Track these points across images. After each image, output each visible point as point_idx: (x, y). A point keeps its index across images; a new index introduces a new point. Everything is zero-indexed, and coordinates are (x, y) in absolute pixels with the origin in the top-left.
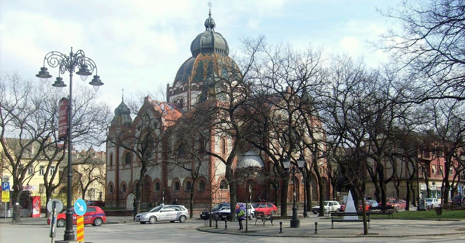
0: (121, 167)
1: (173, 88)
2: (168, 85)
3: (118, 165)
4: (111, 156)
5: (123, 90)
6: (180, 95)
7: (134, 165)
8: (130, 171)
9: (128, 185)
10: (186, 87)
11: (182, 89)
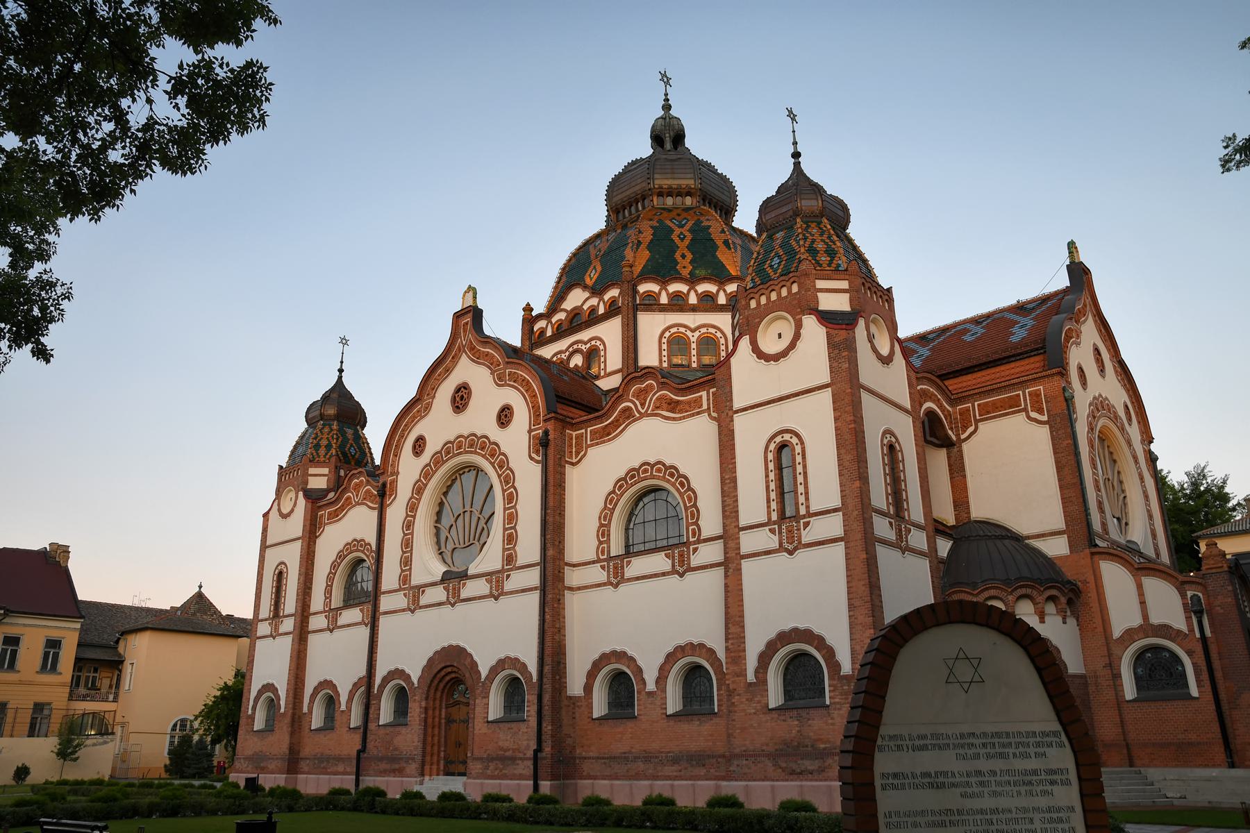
0: (317, 622)
1: (547, 315)
2: (528, 309)
3: (304, 613)
4: (280, 577)
5: (344, 341)
6: (585, 335)
7: (385, 603)
8: (365, 632)
9: (343, 699)
10: (613, 301)
11: (593, 310)
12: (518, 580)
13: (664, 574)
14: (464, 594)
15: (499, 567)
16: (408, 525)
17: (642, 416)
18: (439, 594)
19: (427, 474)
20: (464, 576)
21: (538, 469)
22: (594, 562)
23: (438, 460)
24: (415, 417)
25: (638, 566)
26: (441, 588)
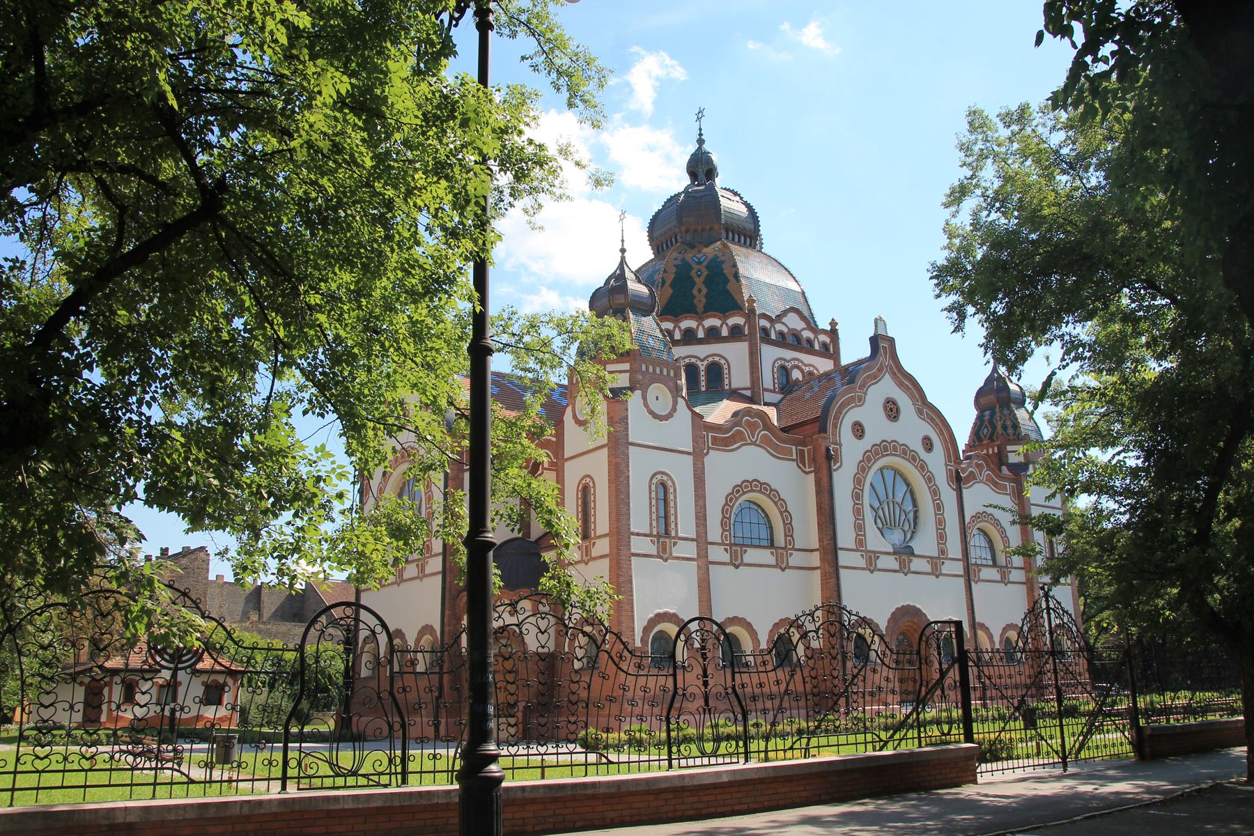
0: (717, 553)
3: (620, 533)
18: (890, 562)
26: (892, 558)
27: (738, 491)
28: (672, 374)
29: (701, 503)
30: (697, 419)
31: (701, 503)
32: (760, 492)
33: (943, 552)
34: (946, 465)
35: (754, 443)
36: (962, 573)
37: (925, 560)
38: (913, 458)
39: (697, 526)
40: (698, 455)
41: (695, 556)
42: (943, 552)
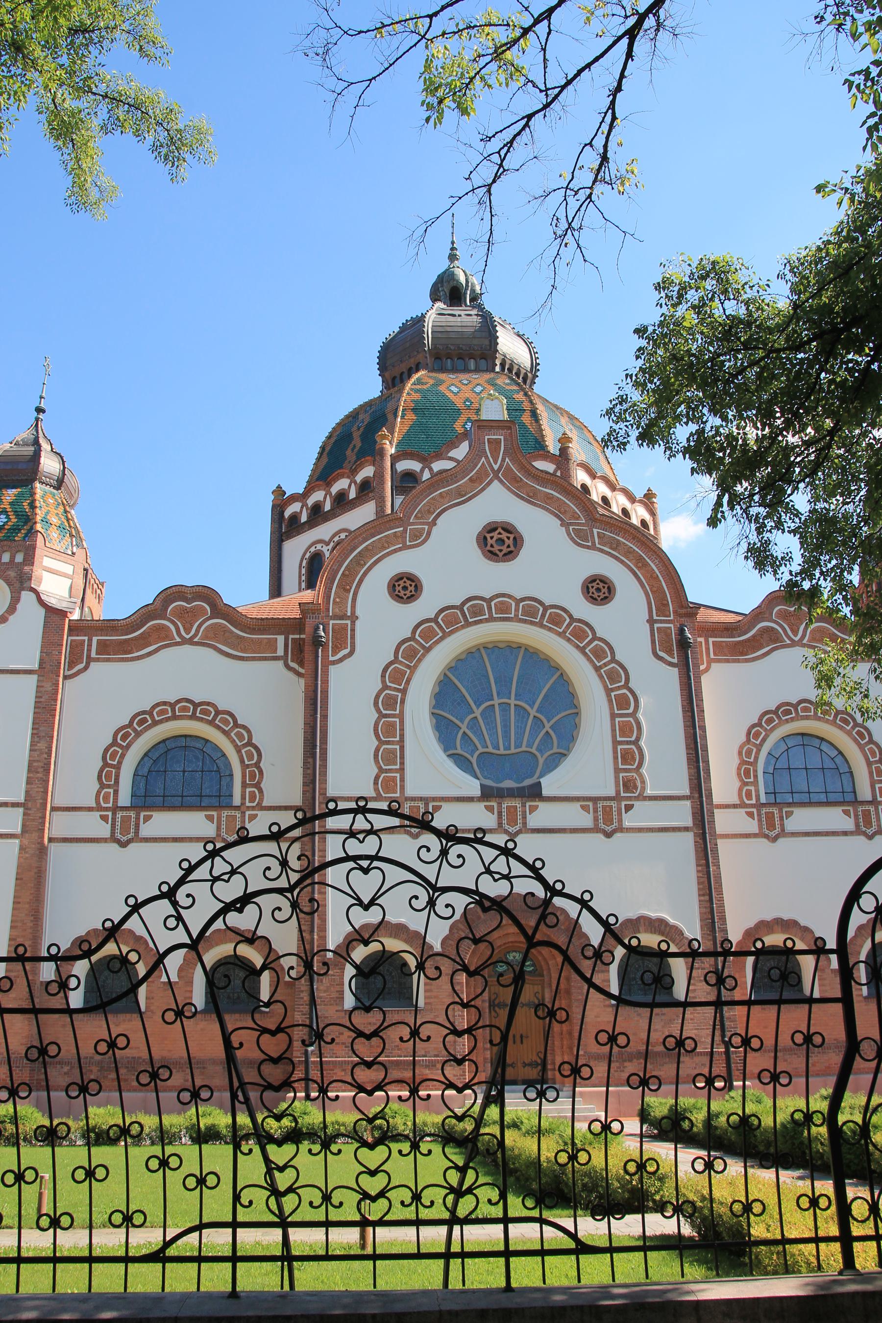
12: (639, 815)
13: (845, 833)
14: (534, 821)
15: (612, 793)
16: (389, 702)
17: (794, 644)
19: (427, 634)
20: (535, 793)
21: (673, 675)
22: (735, 806)
23: (453, 617)
24: (388, 542)
25: (802, 818)
27: (142, 722)
28: (19, 558)
29: (42, 745)
30: (56, 618)
31: (42, 745)
32: (193, 717)
33: (629, 785)
34: (651, 621)
35: (190, 642)
36: (689, 822)
37: (577, 805)
38: (554, 617)
39: (29, 782)
40: (48, 672)
41: (19, 830)
42: (629, 785)
